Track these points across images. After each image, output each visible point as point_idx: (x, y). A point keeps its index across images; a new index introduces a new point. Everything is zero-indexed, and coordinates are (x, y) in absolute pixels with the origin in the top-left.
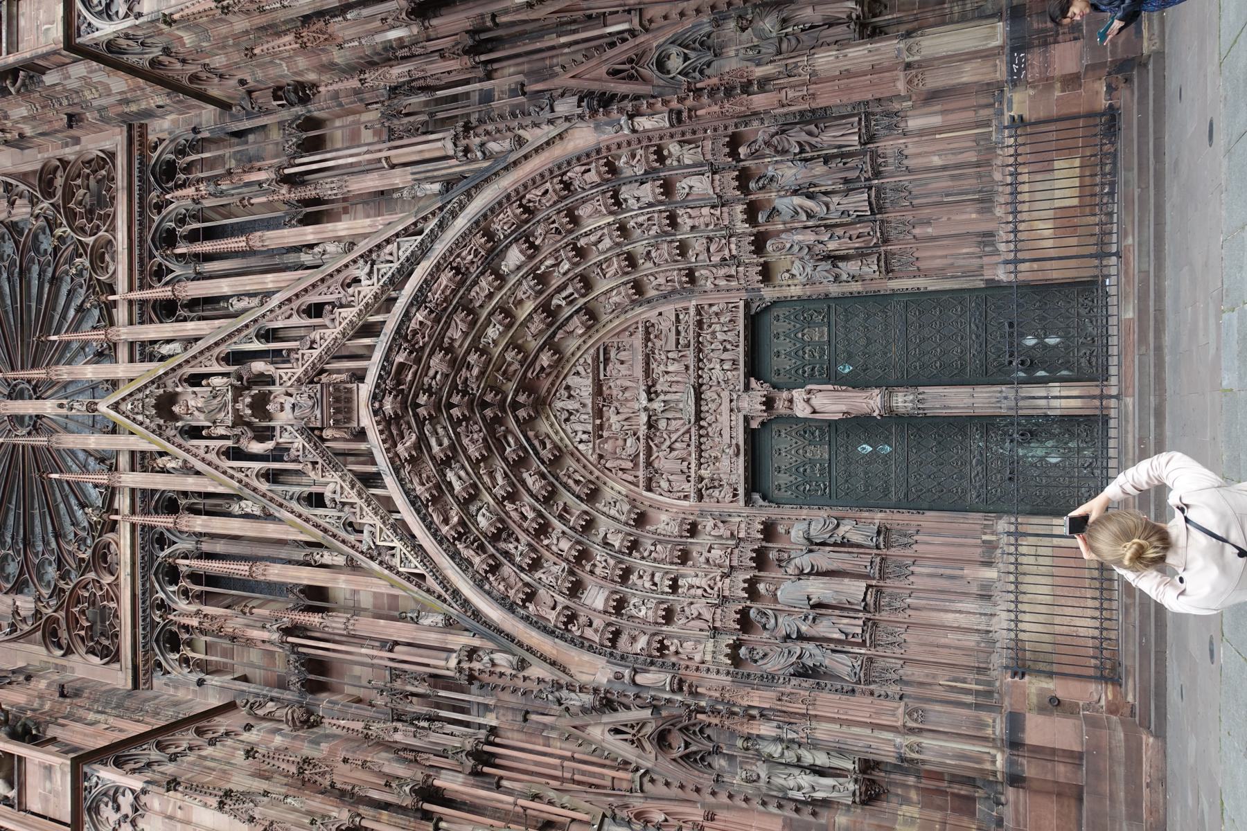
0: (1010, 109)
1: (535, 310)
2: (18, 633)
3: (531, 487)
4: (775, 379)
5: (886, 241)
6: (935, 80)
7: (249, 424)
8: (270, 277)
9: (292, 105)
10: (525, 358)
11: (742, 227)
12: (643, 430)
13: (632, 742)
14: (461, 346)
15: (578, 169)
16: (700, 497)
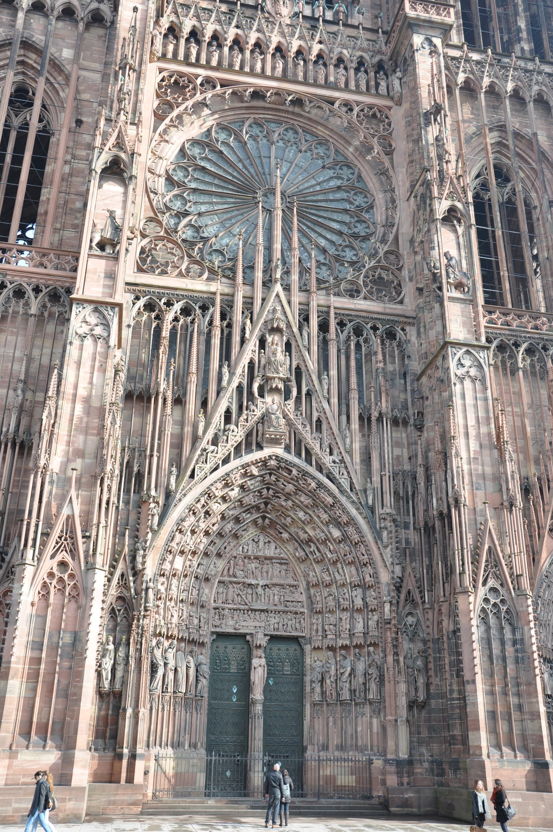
0: (376, 759)
1: (309, 535)
2: (152, 196)
3: (226, 527)
4: (268, 648)
5: (328, 705)
6: (390, 730)
7: (267, 381)
8: (336, 400)
9: (414, 420)
10: (286, 526)
11: (340, 643)
12: (249, 581)
13: (118, 583)
14: (296, 498)
15: (372, 572)
16: (215, 609)
